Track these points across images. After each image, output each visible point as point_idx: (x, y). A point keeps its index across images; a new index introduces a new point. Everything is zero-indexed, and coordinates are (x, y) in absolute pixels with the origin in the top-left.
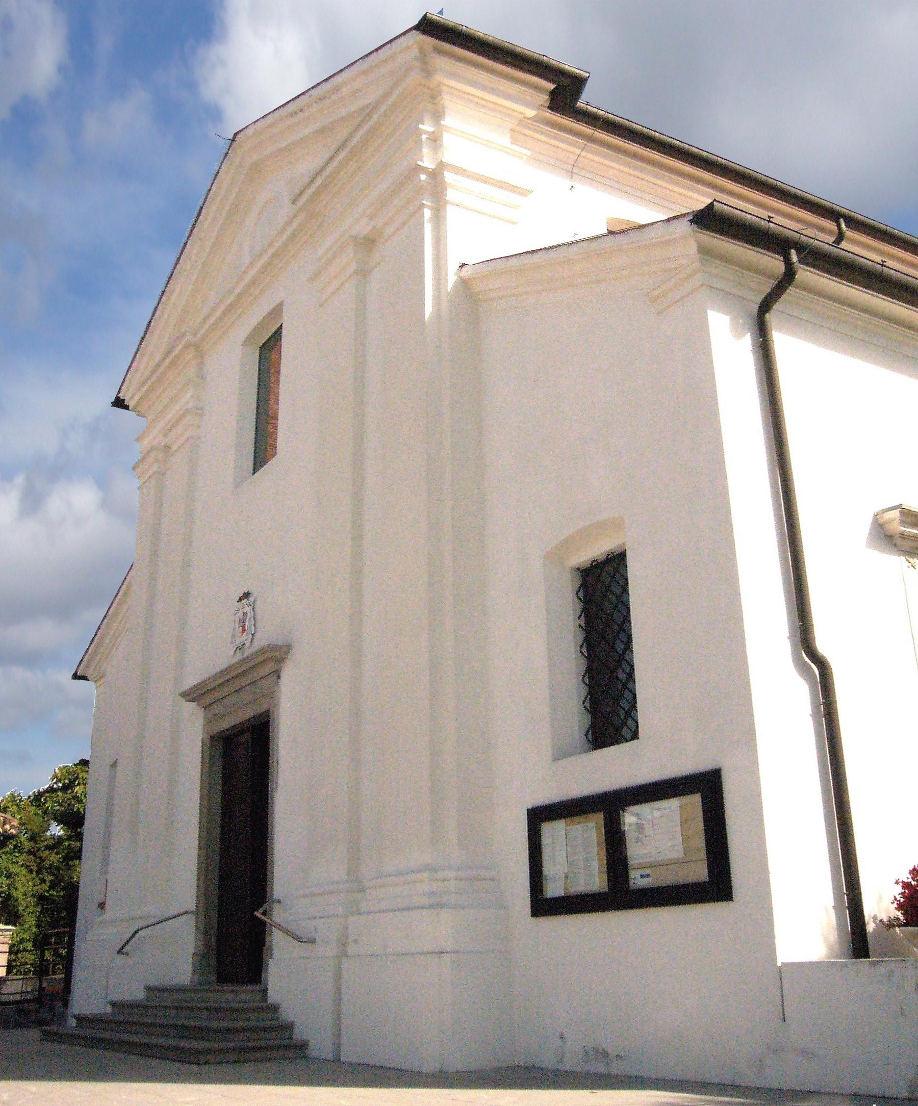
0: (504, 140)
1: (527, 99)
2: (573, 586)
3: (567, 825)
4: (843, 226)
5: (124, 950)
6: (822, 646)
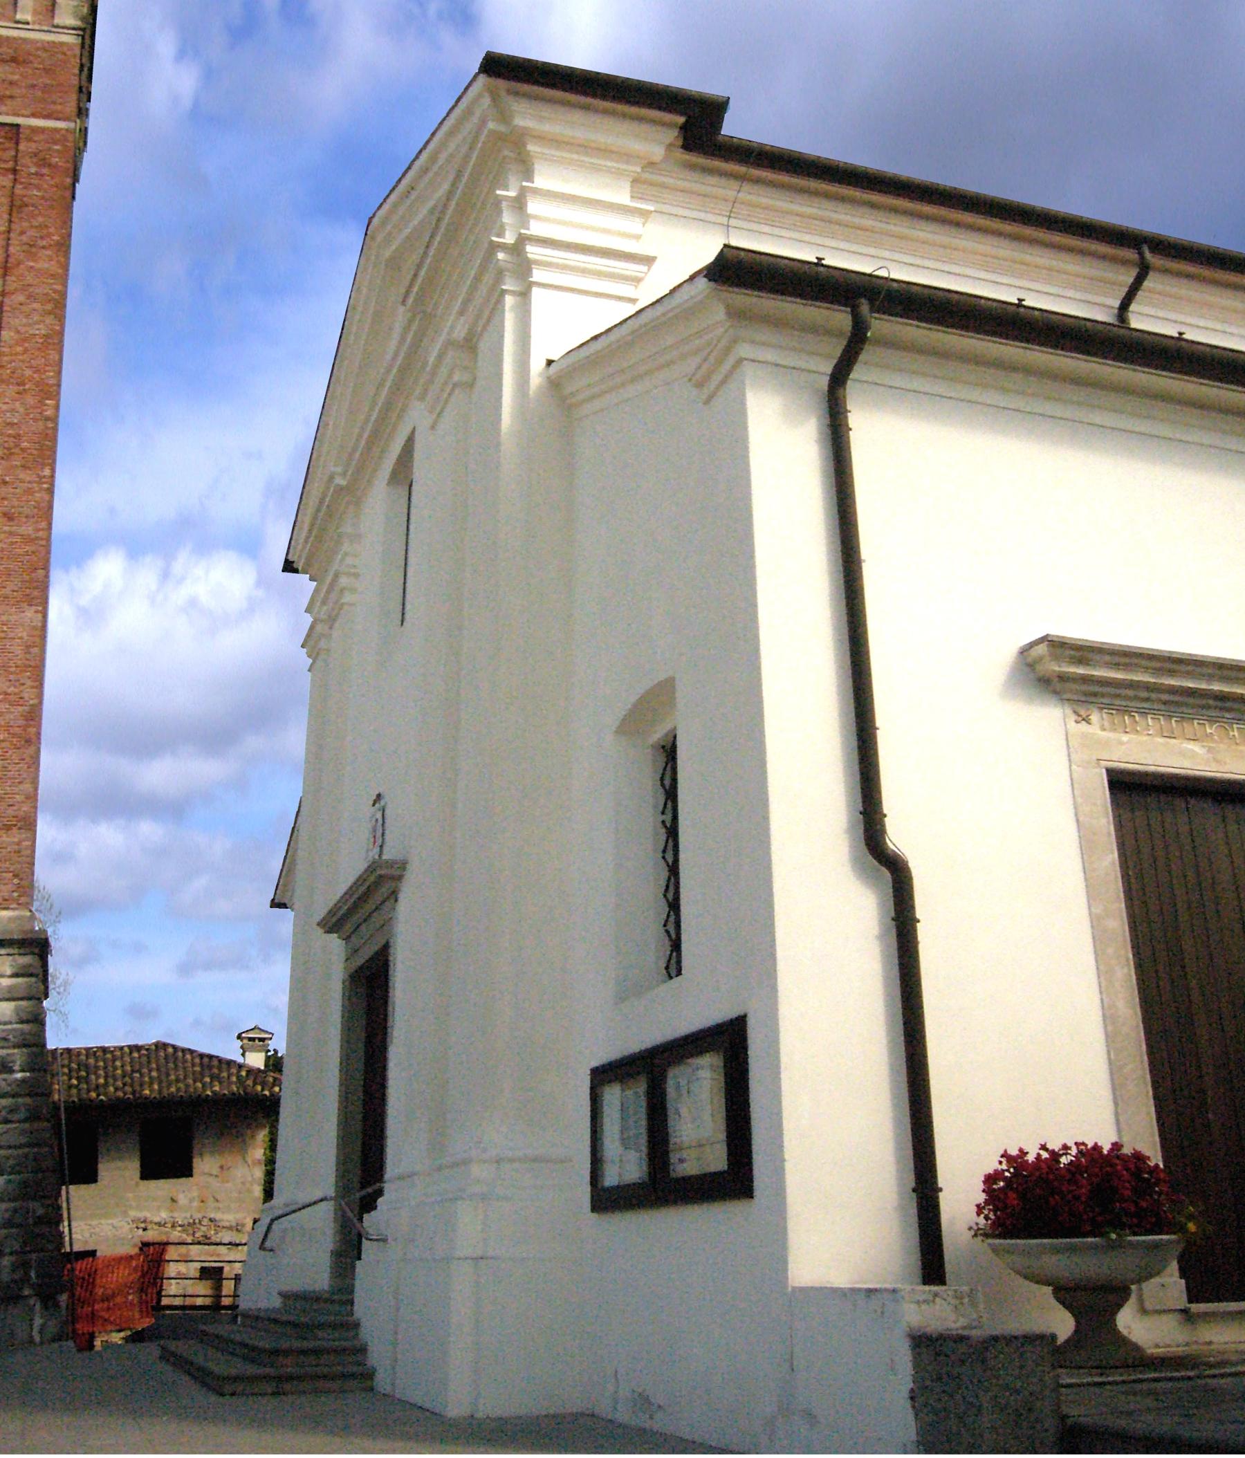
0: (622, 195)
1: (652, 140)
2: (655, 772)
3: (623, 1090)
4: (1148, 255)
5: (268, 1244)
6: (898, 837)
